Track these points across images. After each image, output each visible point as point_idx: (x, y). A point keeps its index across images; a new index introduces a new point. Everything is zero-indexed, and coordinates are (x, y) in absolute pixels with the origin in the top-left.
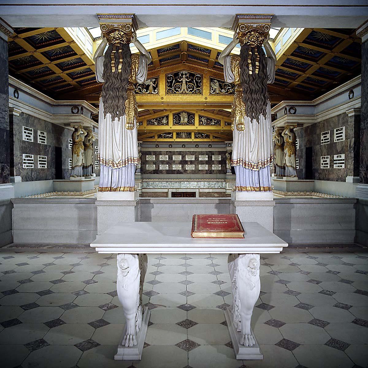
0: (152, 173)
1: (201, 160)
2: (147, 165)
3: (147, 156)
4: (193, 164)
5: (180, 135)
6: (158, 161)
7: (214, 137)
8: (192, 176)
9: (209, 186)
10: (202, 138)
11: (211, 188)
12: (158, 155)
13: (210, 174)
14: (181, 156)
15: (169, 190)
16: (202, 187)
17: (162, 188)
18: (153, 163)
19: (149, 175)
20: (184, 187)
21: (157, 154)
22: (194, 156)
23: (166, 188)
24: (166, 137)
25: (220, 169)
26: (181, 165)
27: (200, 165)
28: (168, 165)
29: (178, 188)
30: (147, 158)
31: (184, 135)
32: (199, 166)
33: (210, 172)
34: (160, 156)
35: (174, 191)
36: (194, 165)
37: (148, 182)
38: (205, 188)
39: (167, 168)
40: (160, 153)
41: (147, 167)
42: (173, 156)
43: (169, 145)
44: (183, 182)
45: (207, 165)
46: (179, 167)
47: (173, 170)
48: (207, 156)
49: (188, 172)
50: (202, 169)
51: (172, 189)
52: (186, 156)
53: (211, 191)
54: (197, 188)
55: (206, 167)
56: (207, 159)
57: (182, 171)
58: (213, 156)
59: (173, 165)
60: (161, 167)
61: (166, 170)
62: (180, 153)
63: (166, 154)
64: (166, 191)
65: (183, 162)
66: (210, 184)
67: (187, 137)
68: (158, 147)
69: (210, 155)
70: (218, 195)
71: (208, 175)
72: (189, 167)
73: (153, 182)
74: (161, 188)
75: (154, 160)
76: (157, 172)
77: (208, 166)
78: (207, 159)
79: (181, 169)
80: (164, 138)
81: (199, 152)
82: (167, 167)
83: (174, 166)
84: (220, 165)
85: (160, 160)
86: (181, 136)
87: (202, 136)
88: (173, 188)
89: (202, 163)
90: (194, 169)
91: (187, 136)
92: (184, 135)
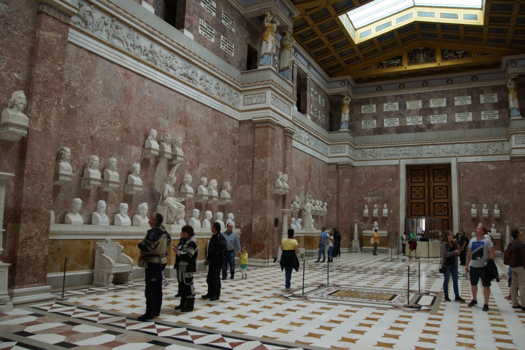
0: (372, 133)
1: (458, 105)
2: (363, 122)
3: (363, 107)
4: (445, 113)
5: (415, 59)
6: (381, 114)
7: (480, 55)
8: (444, 134)
9: (476, 150)
10: (455, 58)
11: (480, 154)
12: (381, 103)
13: (477, 128)
14: (421, 101)
15: (401, 161)
16: (462, 153)
17: (389, 157)
18: (373, 116)
19: (366, 137)
20: (428, 156)
21: (379, 102)
22: (445, 99)
23: (396, 157)
24: (390, 65)
25: (497, 117)
26: (421, 117)
27: (456, 115)
28: (398, 119)
29: (418, 157)
30: (362, 110)
31: (421, 57)
32: (455, 115)
33: (477, 124)
34: (385, 105)
35: (410, 162)
36: (446, 115)
37: (365, 150)
38: (468, 154)
39: (397, 124)
40: (385, 100)
41: (363, 124)
42: (407, 102)
43: (400, 86)
44: (426, 147)
45: (471, 114)
46: (419, 120)
47: (407, 126)
48: (470, 97)
49: (435, 127)
50: (461, 121)
51: (406, 160)
52: (431, 100)
53: (480, 159)
54: (453, 154)
55: (470, 117)
56: (469, 102)
57: (423, 127)
58: (481, 96)
59: (407, 118)
60: (386, 124)
61: (394, 127)
62: (418, 97)
63: (394, 100)
64: (396, 162)
65: (426, 111)
66: (479, 147)
67: (427, 60)
68: (381, 90)
69: (476, 95)
70: (495, 167)
71: (474, 131)
72: (435, 120)
73: (372, 150)
74: (386, 158)
75: (375, 111)
76: (380, 131)
77: (472, 114)
78: (469, 102)
79: (421, 123)
80: (388, 66)
81: (453, 91)
82: (397, 122)
83: (409, 120)
84: (497, 112)
85: (385, 110)
86: (416, 60)
87: (456, 55)
88: (408, 157)
89: (460, 109)
90: (445, 122)
91: (427, 59)
92: (421, 57)
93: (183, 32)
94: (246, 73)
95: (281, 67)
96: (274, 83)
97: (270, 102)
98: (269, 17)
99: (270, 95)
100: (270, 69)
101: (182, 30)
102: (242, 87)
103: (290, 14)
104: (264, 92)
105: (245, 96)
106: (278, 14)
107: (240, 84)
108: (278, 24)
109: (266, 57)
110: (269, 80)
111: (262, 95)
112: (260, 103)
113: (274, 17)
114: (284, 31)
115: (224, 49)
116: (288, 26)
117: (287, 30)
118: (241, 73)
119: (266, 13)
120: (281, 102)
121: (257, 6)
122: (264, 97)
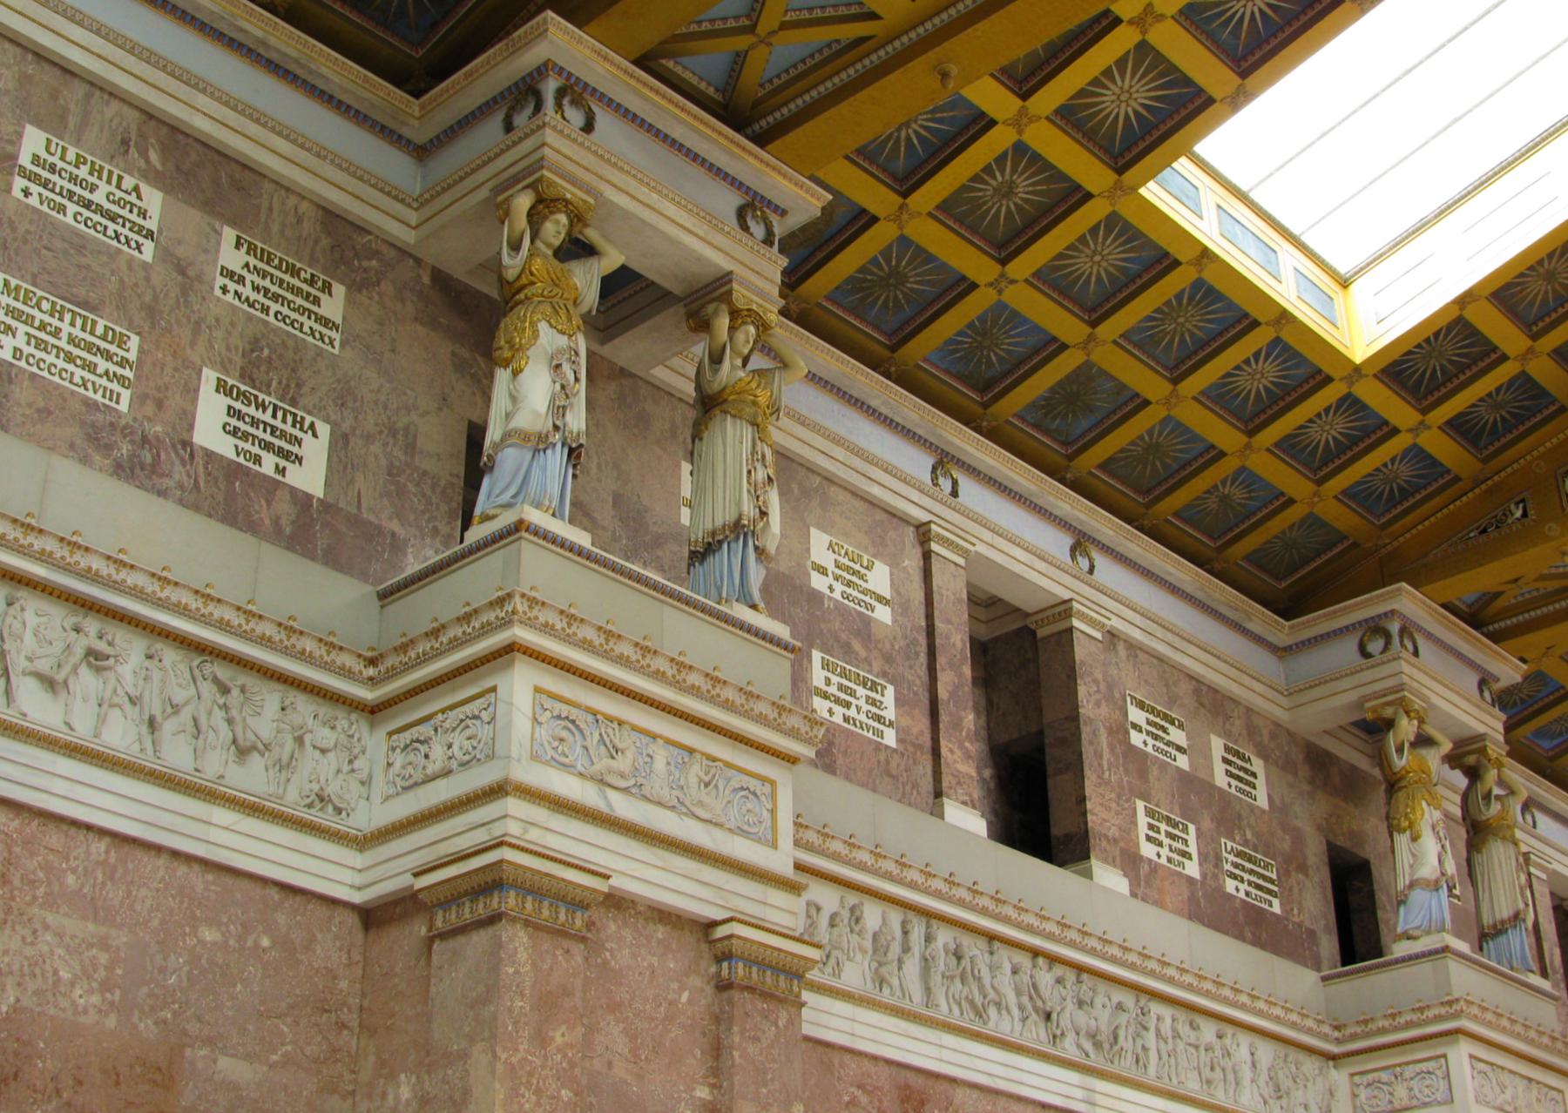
93: (1088, 874)
94: (1339, 975)
95: (1487, 920)
96: (1475, 1010)
97: (1471, 1097)
98: (1407, 728)
99: (1466, 1061)
100: (1446, 949)
101: (1082, 866)
102: (1338, 1041)
103: (1482, 684)
104: (1439, 1052)
105: (1357, 1079)
106: (1435, 699)
107: (1326, 1029)
108: (1447, 746)
109: (1418, 896)
110: (1450, 1003)
111: (1430, 1065)
112: (1425, 1105)
113: (1421, 721)
114: (1471, 760)
115: (1242, 895)
116: (1481, 737)
117: (1483, 751)
118: (1324, 979)
119: (1388, 712)
120: (1518, 1081)
121: (1347, 683)
122: (1438, 1073)
